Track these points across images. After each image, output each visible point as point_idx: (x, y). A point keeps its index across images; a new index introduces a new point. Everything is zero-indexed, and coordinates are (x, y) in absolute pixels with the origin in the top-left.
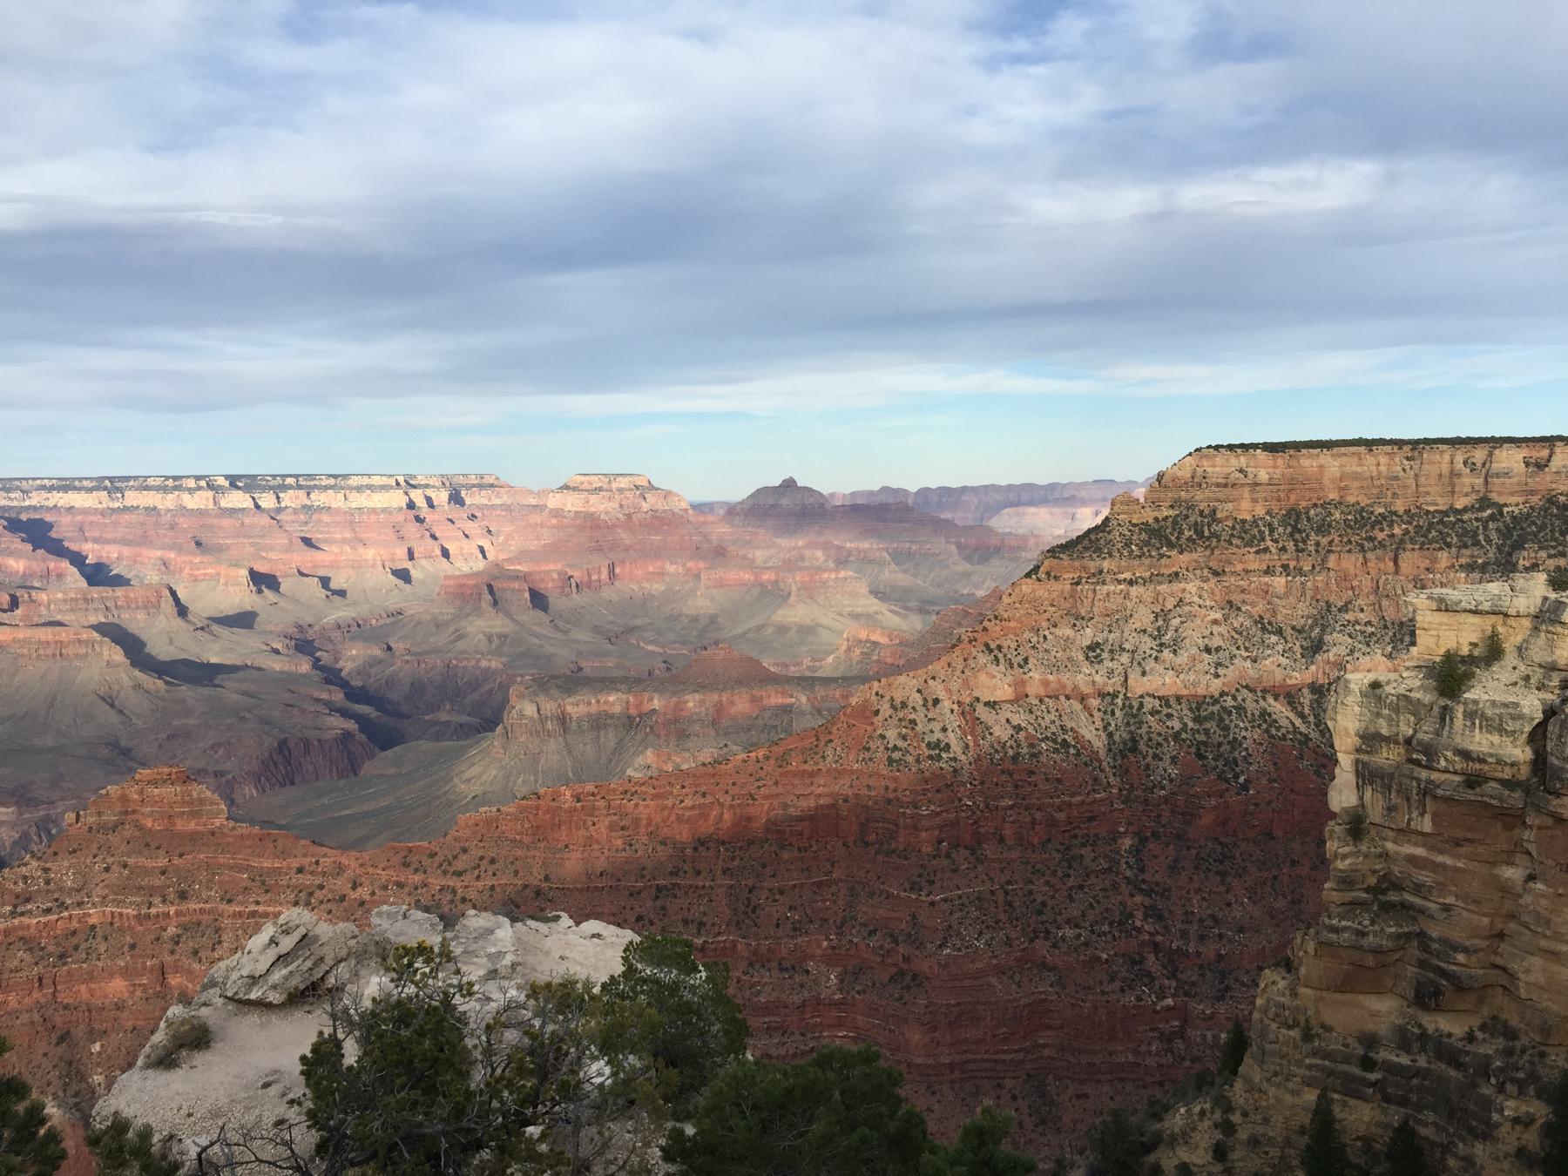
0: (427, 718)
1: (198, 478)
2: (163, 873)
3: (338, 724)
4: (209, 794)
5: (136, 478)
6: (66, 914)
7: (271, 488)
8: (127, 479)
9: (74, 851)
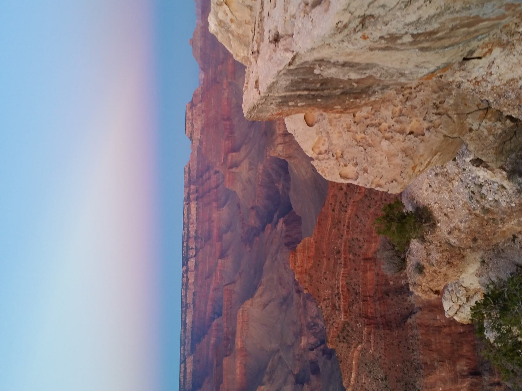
0: (281, 193)
1: (183, 277)
2: (329, 259)
3: (281, 225)
4: (301, 243)
5: (182, 299)
6: (341, 292)
7: (187, 251)
8: (182, 302)
9: (318, 291)
